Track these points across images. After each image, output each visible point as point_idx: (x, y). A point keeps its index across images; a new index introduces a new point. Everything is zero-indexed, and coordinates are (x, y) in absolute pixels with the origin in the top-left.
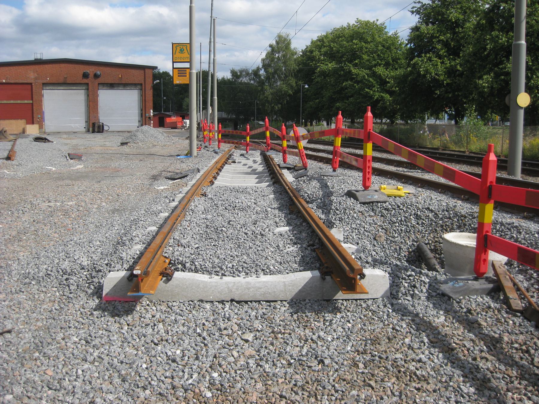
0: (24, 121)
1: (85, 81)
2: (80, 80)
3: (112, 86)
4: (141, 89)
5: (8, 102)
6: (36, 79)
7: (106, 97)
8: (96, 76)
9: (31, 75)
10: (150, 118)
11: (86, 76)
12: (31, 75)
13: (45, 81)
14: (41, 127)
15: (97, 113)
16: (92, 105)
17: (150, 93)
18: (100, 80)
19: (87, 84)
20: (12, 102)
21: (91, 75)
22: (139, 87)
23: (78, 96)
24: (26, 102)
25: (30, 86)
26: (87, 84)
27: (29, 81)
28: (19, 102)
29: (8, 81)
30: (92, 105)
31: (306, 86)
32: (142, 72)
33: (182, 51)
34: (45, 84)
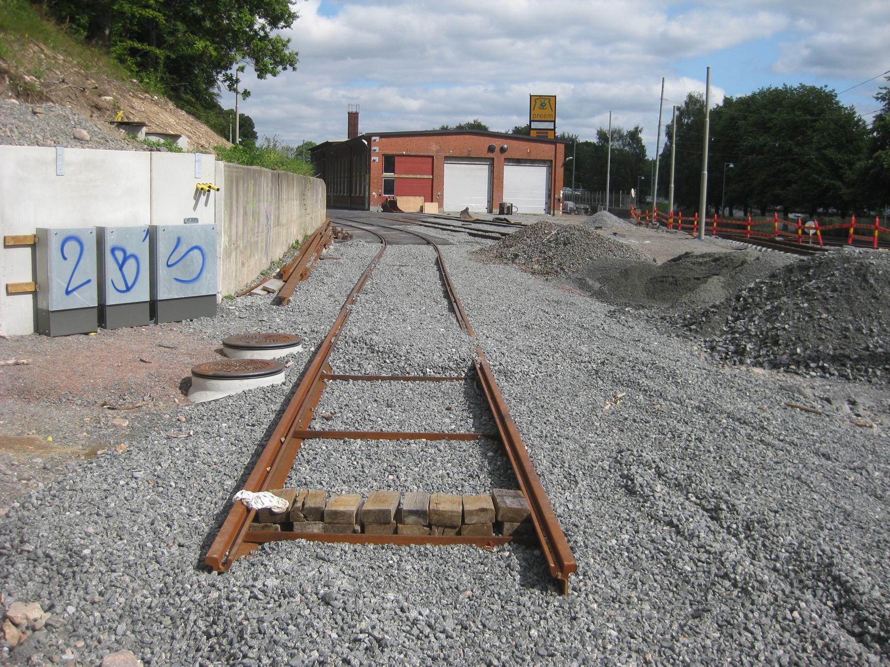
0: (422, 198)
1: (491, 155)
2: (485, 153)
3: (518, 162)
4: (550, 167)
5: (422, 177)
6: (438, 151)
7: (512, 175)
8: (503, 150)
9: (432, 146)
10: (559, 200)
11: (491, 149)
12: (432, 146)
13: (447, 155)
14: (441, 205)
15: (502, 192)
16: (495, 184)
17: (560, 171)
18: (506, 155)
19: (493, 159)
20: (411, 176)
21: (497, 149)
22: (549, 163)
23: (482, 171)
24: (426, 177)
25: (430, 159)
26: (493, 159)
27: (431, 154)
28: (418, 176)
29: (408, 153)
30: (495, 184)
31: (732, 166)
32: (553, 146)
33: (543, 106)
34: (448, 158)
